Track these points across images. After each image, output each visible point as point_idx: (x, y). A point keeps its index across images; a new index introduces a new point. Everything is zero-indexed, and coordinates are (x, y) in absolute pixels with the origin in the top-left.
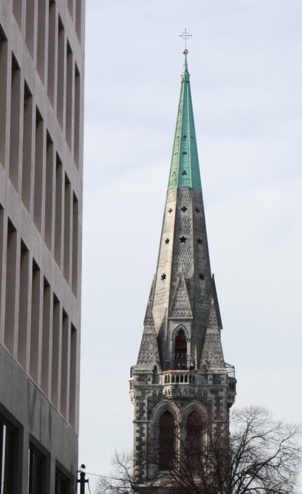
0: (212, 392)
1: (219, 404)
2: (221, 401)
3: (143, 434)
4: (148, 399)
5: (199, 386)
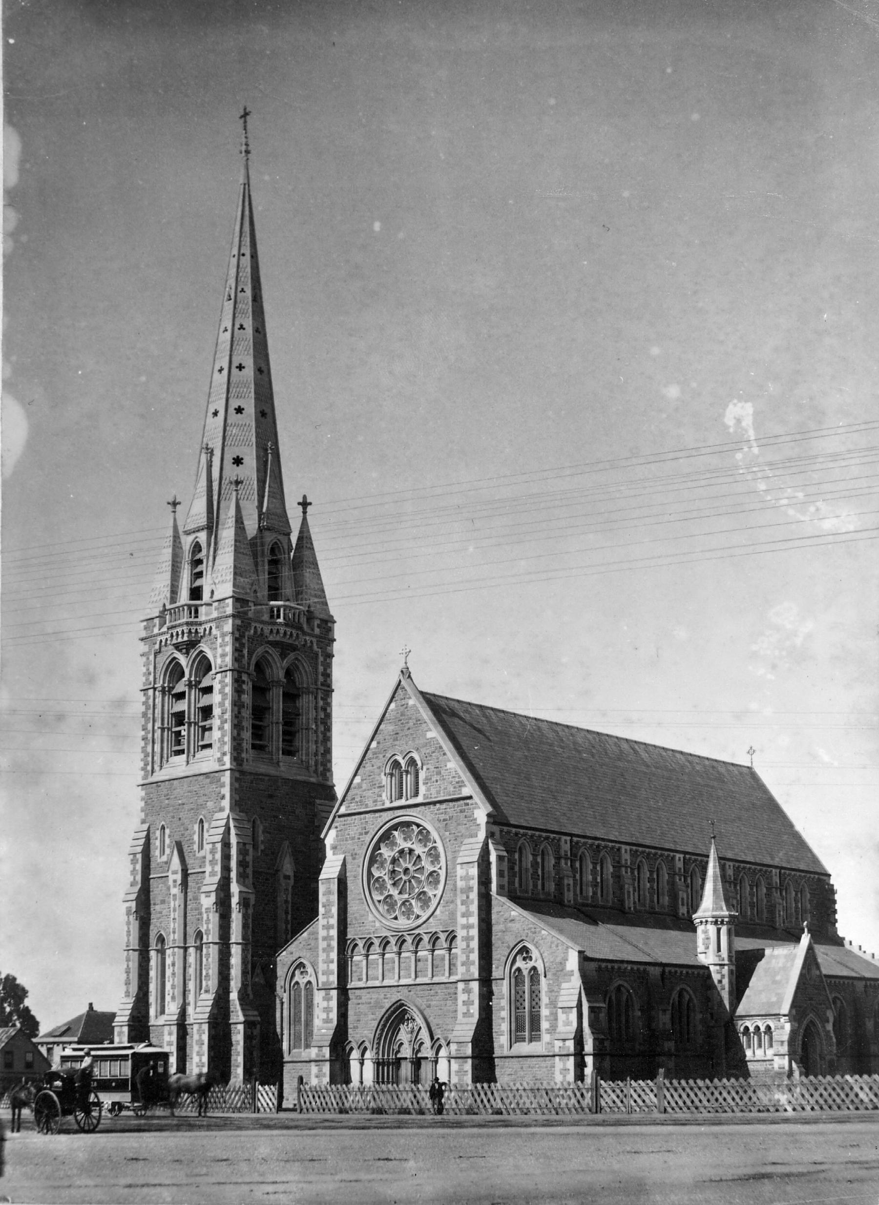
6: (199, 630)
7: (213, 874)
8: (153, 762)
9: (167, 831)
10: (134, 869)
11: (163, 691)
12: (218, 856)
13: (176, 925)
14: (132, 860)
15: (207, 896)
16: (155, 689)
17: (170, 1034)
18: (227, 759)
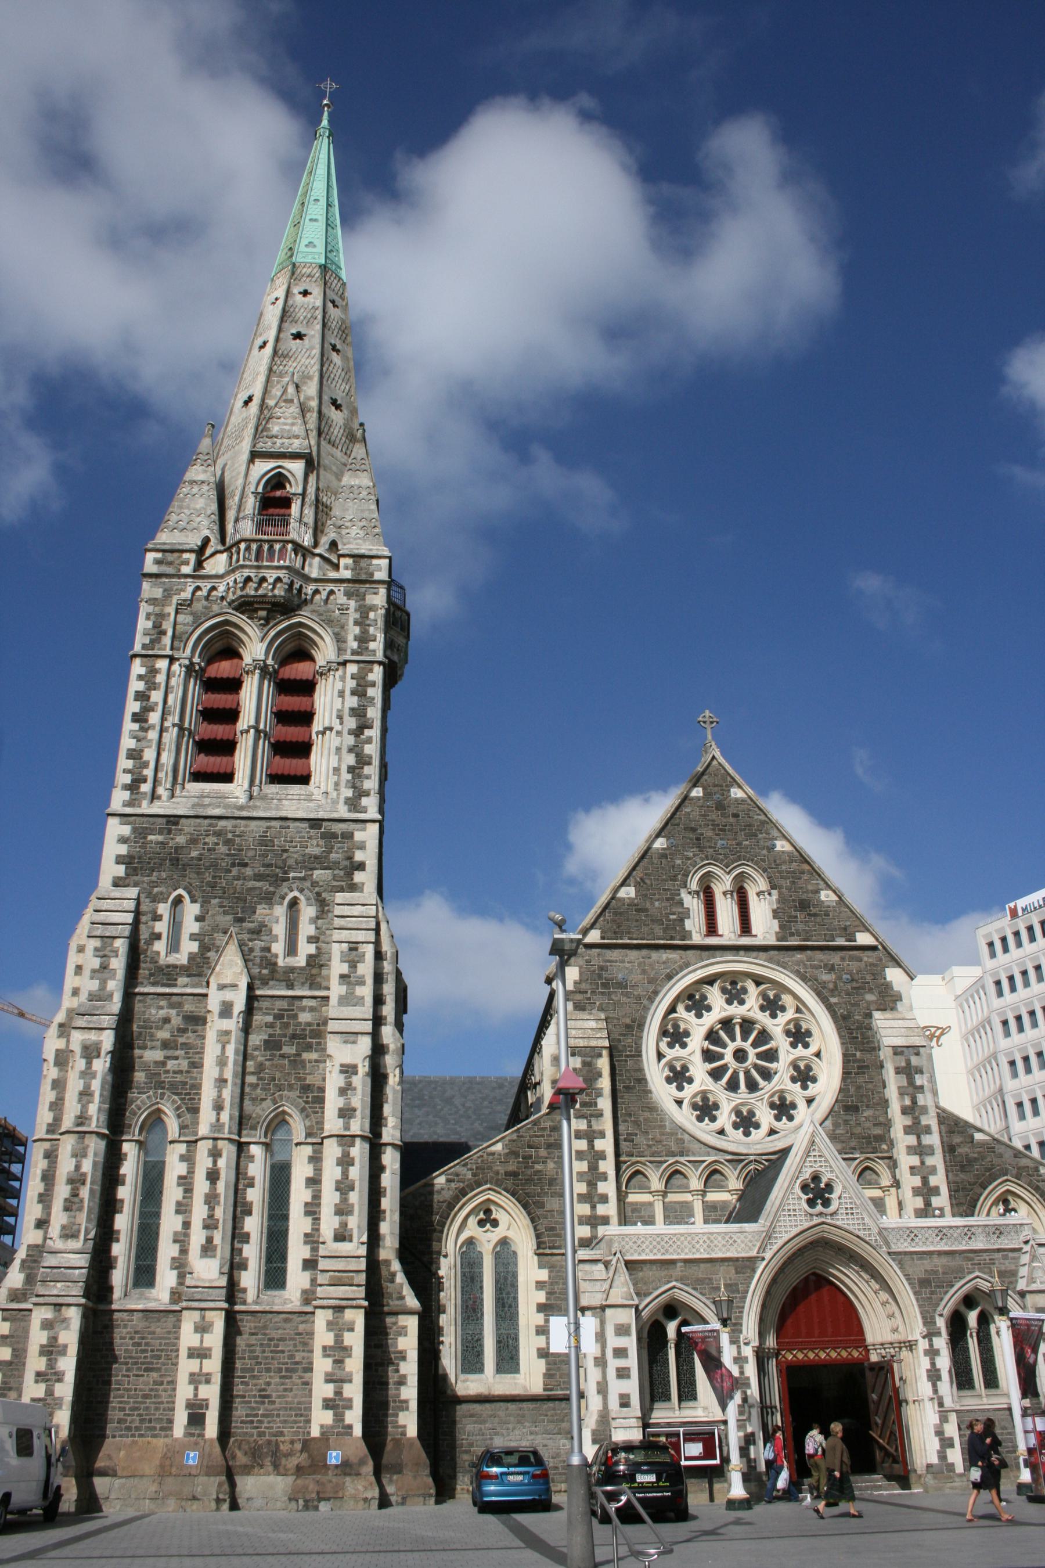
0: (349, 595)
1: (368, 622)
2: (372, 615)
3: (155, 683)
4: (178, 604)
5: (316, 580)
6: (304, 590)
7: (346, 1000)
8: (156, 781)
10: (104, 967)
11: (190, 669)
12: (366, 968)
14: (96, 949)
15: (345, 1042)
16: (172, 660)
17: (202, 1328)
18: (371, 805)
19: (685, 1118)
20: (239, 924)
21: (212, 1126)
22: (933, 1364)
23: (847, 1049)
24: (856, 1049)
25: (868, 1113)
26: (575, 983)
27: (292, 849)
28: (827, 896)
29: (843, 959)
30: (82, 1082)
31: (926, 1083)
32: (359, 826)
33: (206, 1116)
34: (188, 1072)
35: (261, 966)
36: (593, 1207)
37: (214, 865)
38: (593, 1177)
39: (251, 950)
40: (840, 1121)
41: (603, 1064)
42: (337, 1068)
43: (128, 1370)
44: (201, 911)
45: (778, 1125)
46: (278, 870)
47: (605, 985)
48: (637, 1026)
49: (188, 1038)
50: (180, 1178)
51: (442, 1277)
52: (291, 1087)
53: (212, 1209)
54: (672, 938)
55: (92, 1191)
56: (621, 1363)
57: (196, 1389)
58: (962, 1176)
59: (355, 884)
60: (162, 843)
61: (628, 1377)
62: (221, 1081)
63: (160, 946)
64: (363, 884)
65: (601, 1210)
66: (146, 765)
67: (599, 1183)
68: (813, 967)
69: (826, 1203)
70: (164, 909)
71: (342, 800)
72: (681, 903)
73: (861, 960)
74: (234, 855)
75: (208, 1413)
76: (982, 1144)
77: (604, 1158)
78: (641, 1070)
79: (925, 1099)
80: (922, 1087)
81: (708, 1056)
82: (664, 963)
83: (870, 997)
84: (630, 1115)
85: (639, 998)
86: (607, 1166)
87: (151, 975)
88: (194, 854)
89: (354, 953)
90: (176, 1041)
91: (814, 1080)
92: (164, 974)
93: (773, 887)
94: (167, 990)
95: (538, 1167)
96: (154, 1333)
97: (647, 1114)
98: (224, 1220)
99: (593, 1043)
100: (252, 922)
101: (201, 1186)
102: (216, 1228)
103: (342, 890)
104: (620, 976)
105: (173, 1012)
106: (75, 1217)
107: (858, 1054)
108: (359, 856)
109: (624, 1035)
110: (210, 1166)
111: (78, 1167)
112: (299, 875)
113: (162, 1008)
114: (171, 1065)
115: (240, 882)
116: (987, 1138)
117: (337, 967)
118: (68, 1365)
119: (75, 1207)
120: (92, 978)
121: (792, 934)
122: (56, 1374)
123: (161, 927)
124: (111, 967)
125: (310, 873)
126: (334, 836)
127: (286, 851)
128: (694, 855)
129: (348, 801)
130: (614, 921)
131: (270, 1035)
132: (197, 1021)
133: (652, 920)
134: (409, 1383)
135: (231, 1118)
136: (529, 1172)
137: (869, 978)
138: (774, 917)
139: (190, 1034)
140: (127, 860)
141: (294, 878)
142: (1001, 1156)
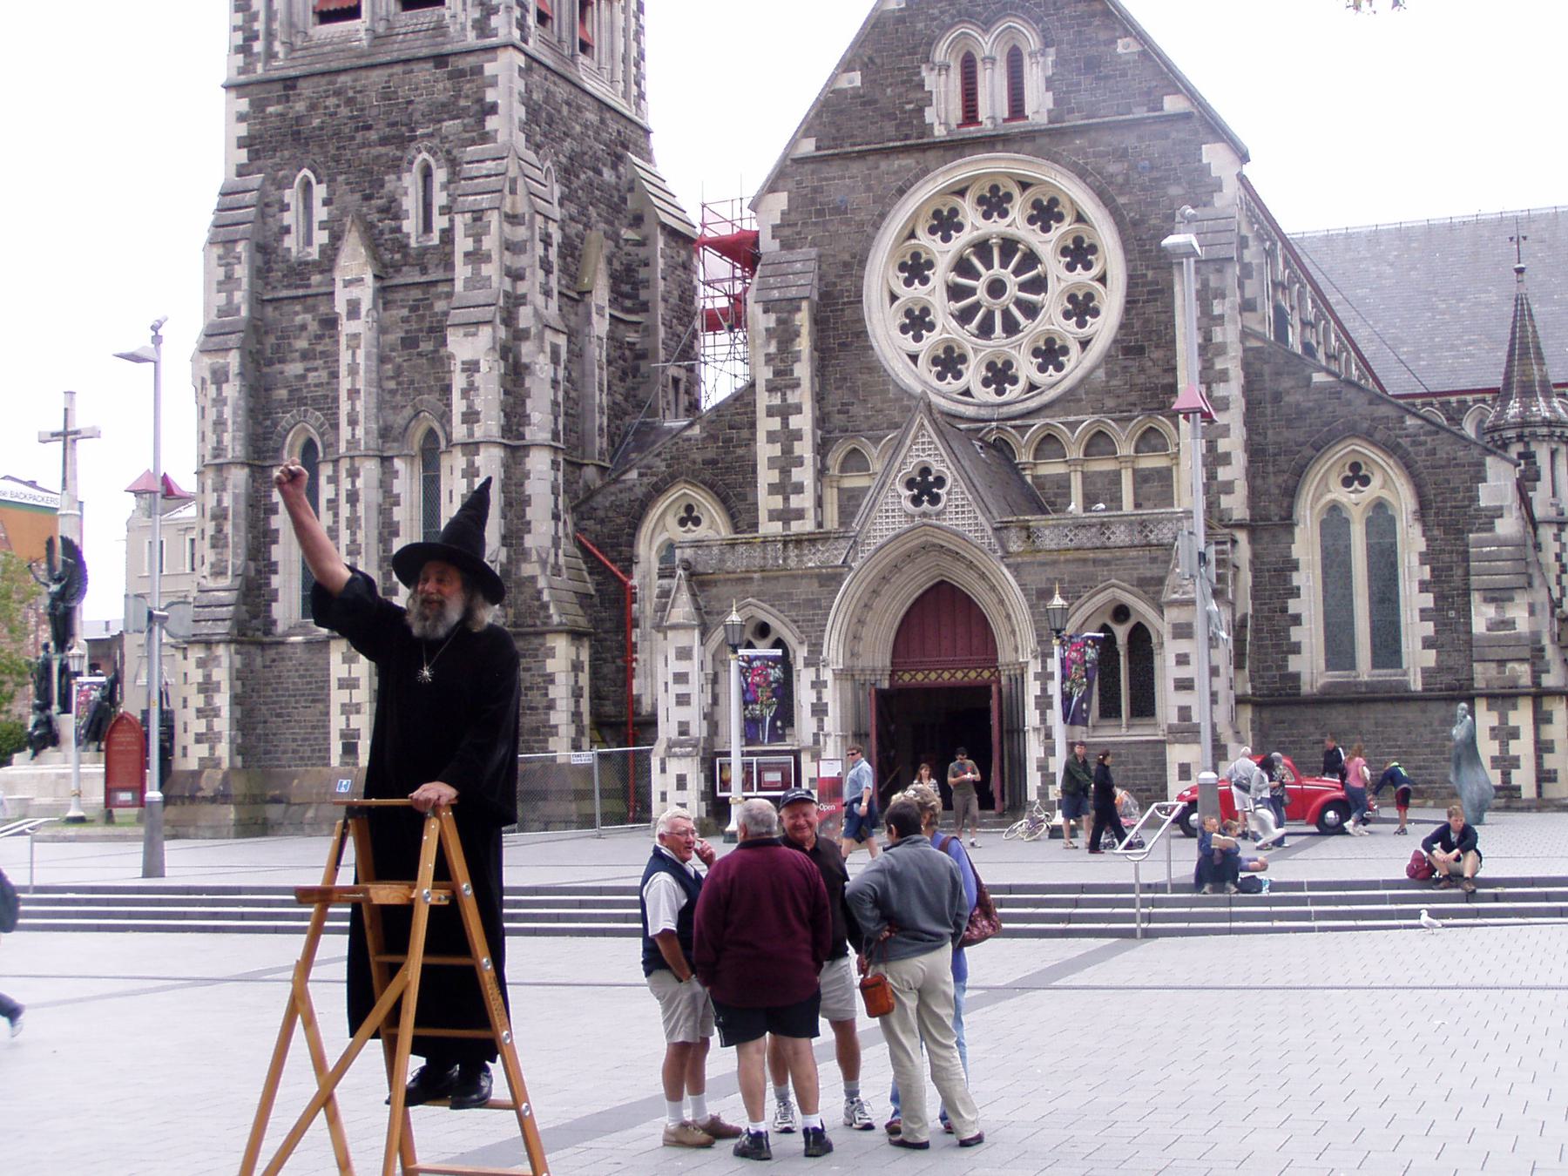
7: (475, 282)
8: (270, 35)
9: (320, 191)
10: (229, 277)
12: (490, 243)
13: (360, 406)
15: (466, 335)
19: (916, 378)
20: (366, 204)
21: (348, 442)
22: (1044, 690)
23: (1135, 269)
24: (1147, 267)
25: (1157, 354)
26: (783, 213)
27: (417, 99)
28: (1127, 46)
29: (1141, 138)
30: (214, 409)
31: (1228, 313)
32: (489, 56)
33: (345, 432)
34: (328, 383)
35: (392, 251)
36: (786, 499)
37: (337, 134)
38: (787, 462)
39: (382, 233)
40: (1117, 369)
41: (803, 319)
42: (459, 366)
43: (296, 702)
44: (328, 193)
45: (1039, 378)
46: (404, 129)
47: (820, 213)
48: (857, 263)
49: (326, 345)
50: (329, 501)
51: (635, 588)
52: (430, 390)
53: (353, 534)
54: (907, 137)
55: (235, 526)
56: (681, 689)
57: (348, 719)
58: (1287, 434)
59: (487, 133)
60: (281, 115)
61: (688, 703)
62: (353, 393)
63: (290, 242)
64: (496, 131)
65: (795, 502)
66: (254, 17)
67: (793, 470)
68: (1096, 155)
69: (935, 500)
70: (291, 196)
71: (469, 24)
72: (921, 85)
73: (1167, 137)
74: (358, 117)
75: (360, 742)
76: (1322, 388)
77: (800, 438)
78: (861, 320)
79: (1224, 335)
80: (1221, 317)
81: (956, 292)
82: (895, 173)
83: (1174, 191)
84: (845, 379)
85: (862, 224)
86: (804, 449)
87: (284, 276)
88: (316, 122)
89: (479, 223)
90: (314, 350)
91: (1095, 313)
92: (297, 274)
93: (1047, 45)
94: (300, 292)
95: (740, 451)
96: (316, 664)
97: (864, 377)
98: (367, 544)
99: (792, 293)
100: (381, 198)
101: (345, 510)
102: (359, 553)
103: (473, 142)
104: (839, 198)
105: (309, 317)
106: (221, 554)
107: (1150, 274)
108: (491, 95)
109: (841, 276)
110: (349, 487)
111: (219, 501)
112: (426, 131)
113: (297, 314)
114: (312, 377)
115: (364, 151)
116: (1331, 379)
117: (463, 244)
118: (223, 700)
119: (221, 543)
120: (219, 291)
121: (1071, 111)
122: (213, 709)
123: (288, 218)
124: (236, 276)
125: (438, 126)
126: (461, 73)
127: (410, 102)
128: (942, 13)
129: (475, 21)
130: (833, 123)
131: (407, 332)
132: (330, 323)
133: (882, 116)
134: (558, 708)
135: (367, 433)
136: (729, 458)
137: (1176, 162)
138: (1048, 89)
139: (327, 340)
140: (248, 142)
141: (423, 136)
142: (1349, 403)
